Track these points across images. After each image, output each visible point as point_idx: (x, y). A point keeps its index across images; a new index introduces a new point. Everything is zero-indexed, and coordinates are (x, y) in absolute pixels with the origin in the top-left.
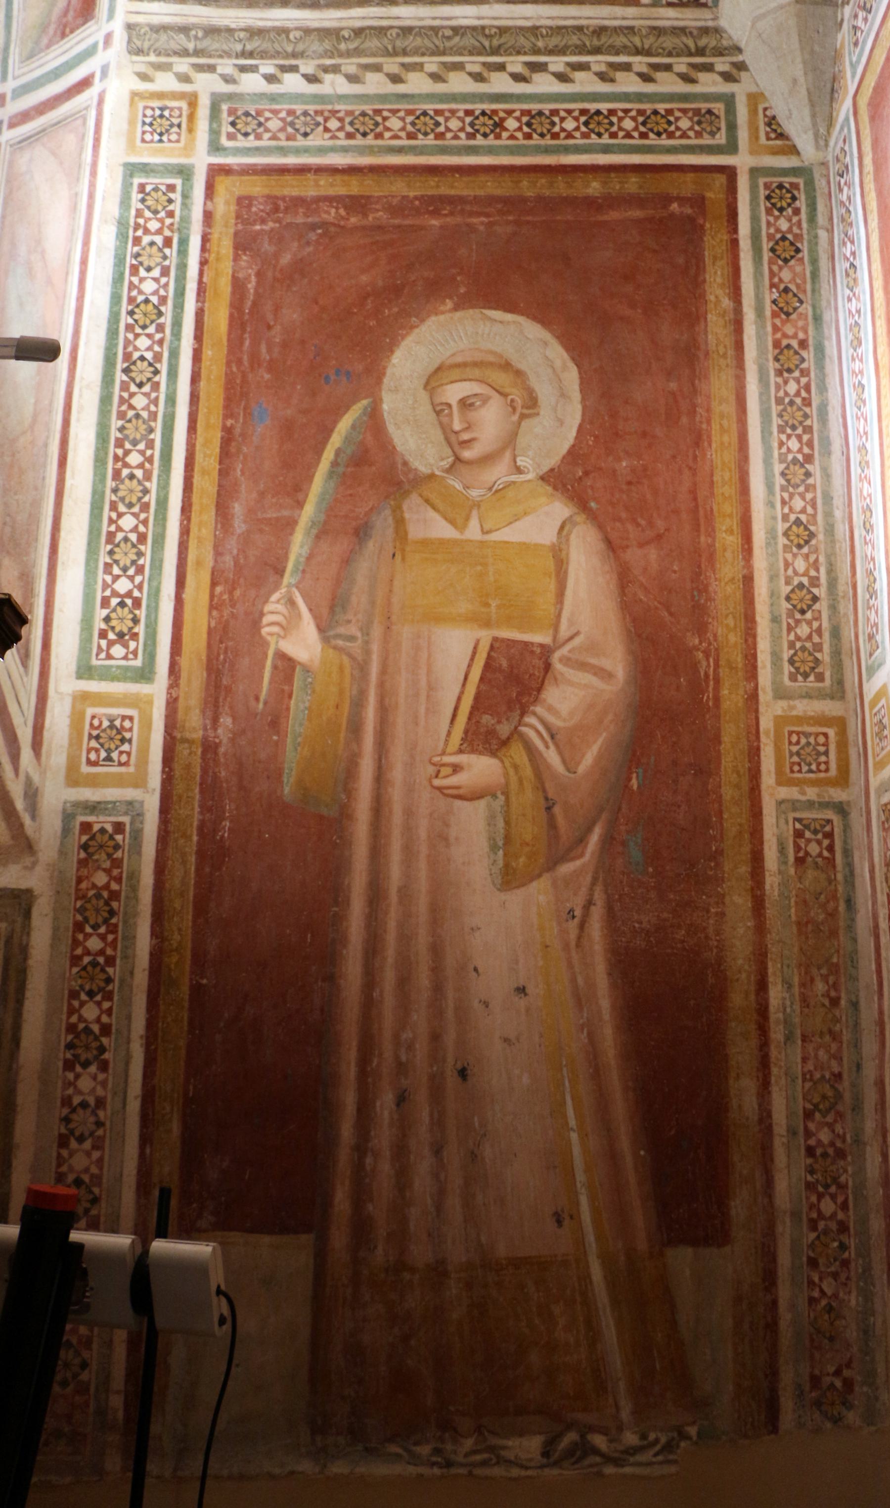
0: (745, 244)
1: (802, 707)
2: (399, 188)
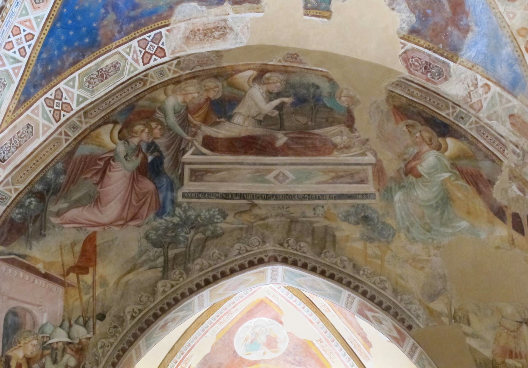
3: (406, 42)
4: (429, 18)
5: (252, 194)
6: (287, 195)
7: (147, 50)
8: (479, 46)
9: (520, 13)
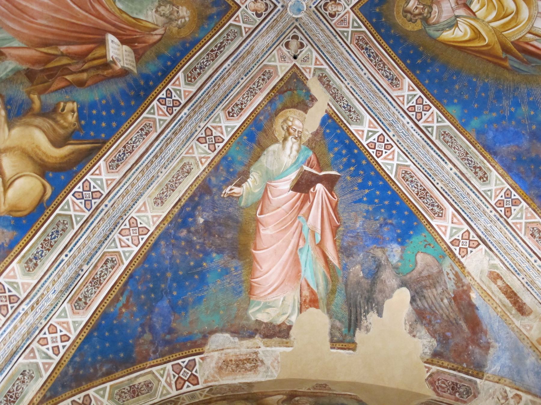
3: (430, 366)
4: (450, 341)
7: (181, 375)
8: (503, 360)
9: (535, 325)
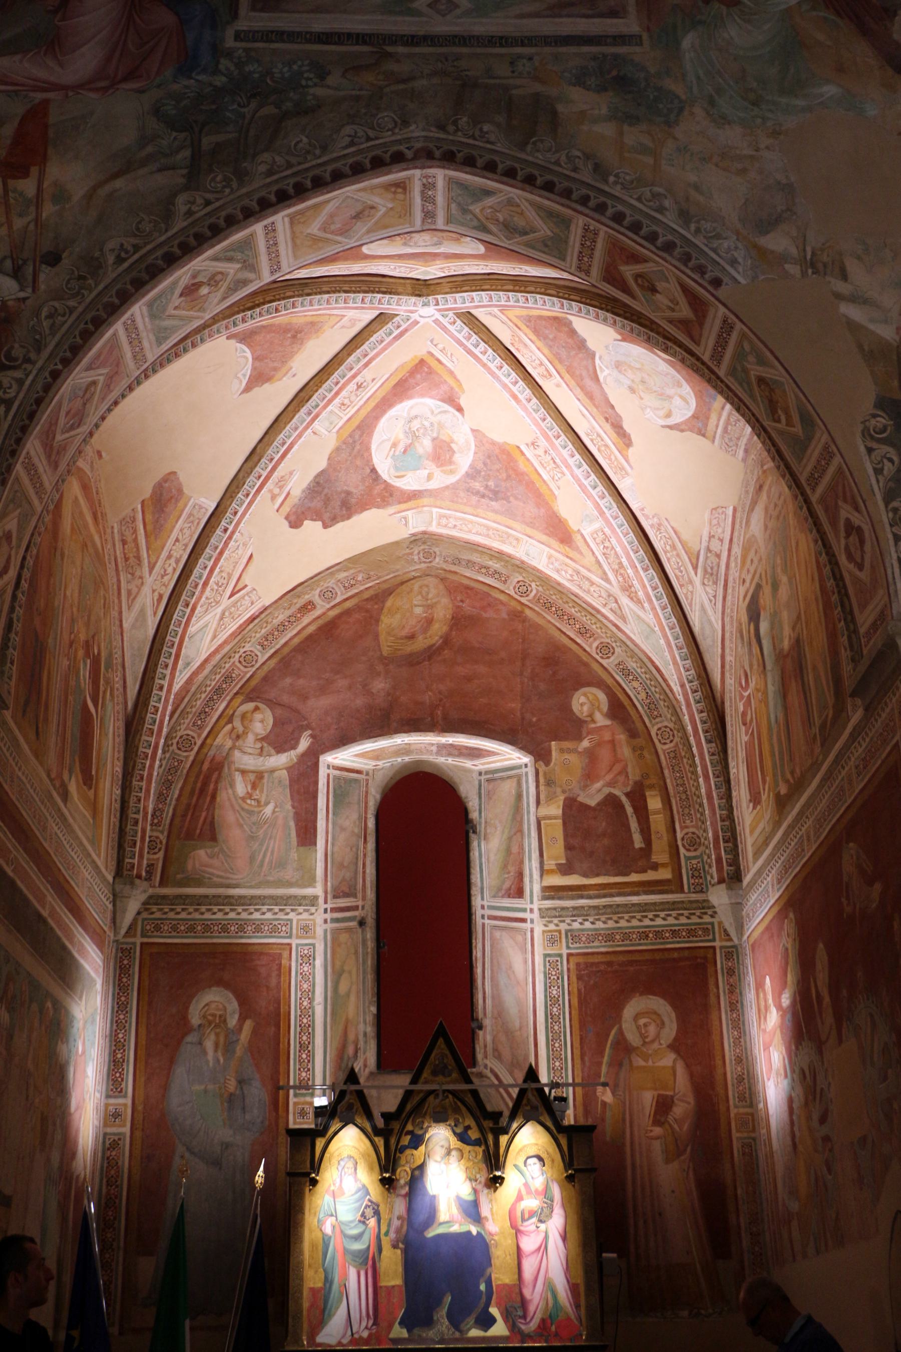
0: (719, 971)
1: (742, 1110)
2: (621, 958)
5: (382, 35)
6: (456, 36)
